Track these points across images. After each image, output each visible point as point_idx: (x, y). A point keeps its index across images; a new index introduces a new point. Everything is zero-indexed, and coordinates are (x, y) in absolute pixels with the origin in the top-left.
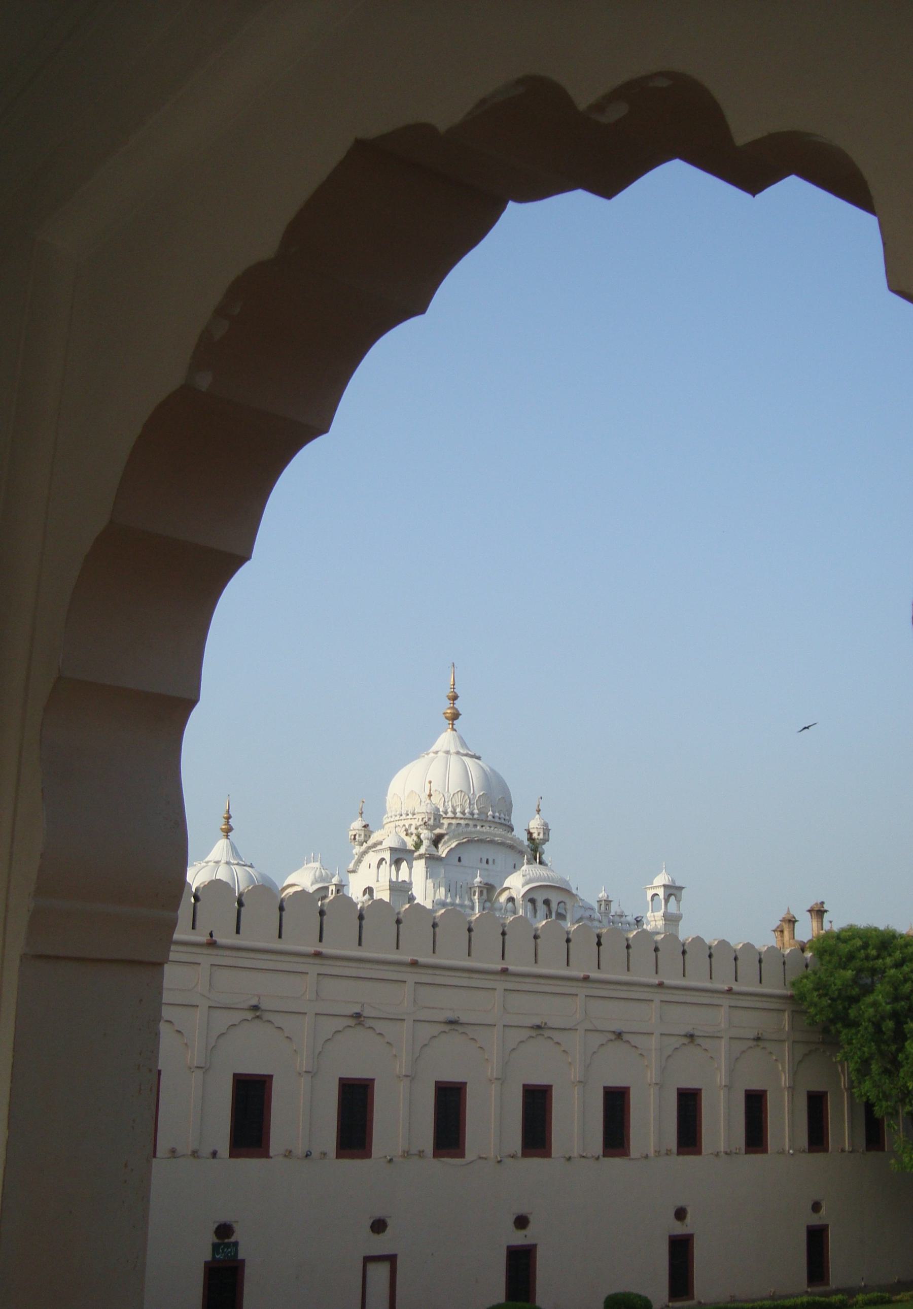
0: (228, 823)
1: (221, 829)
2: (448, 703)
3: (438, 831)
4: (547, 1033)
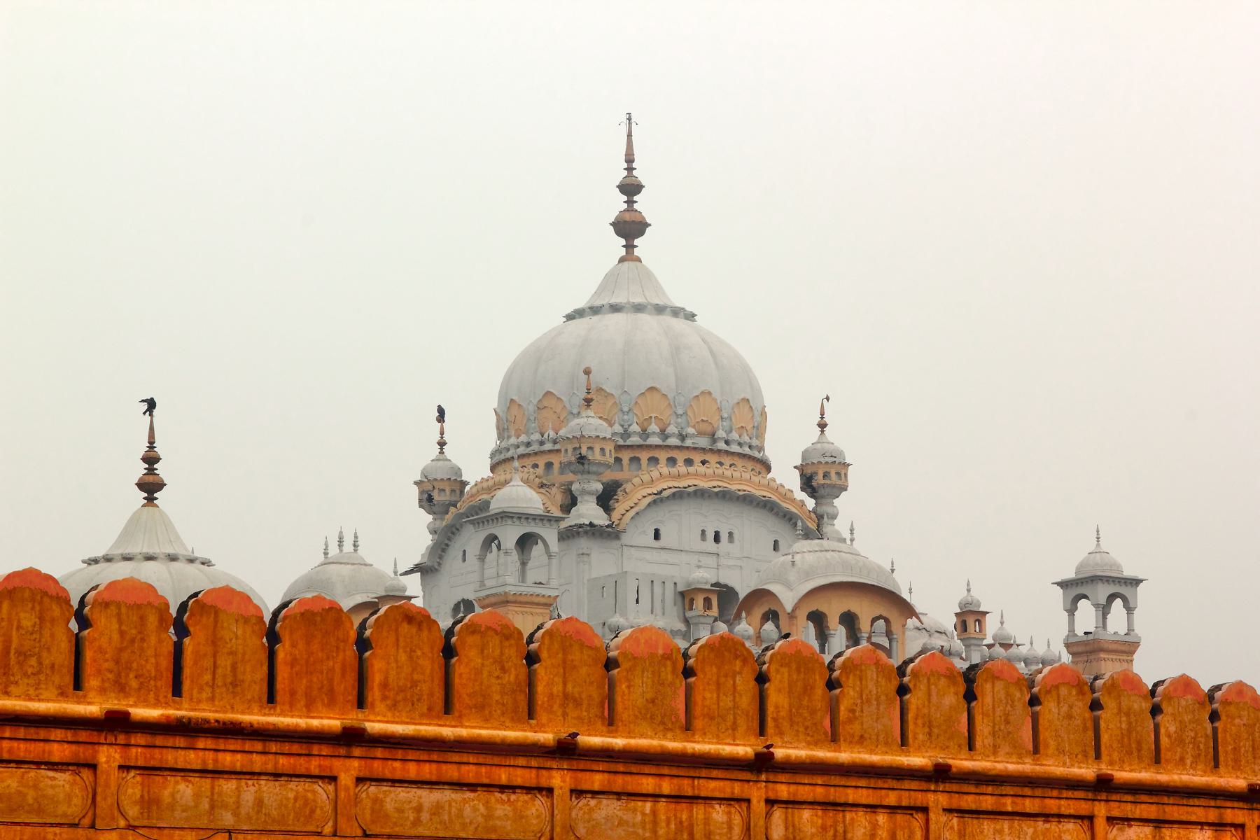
0: (151, 471)
2: (620, 202)
3: (610, 476)
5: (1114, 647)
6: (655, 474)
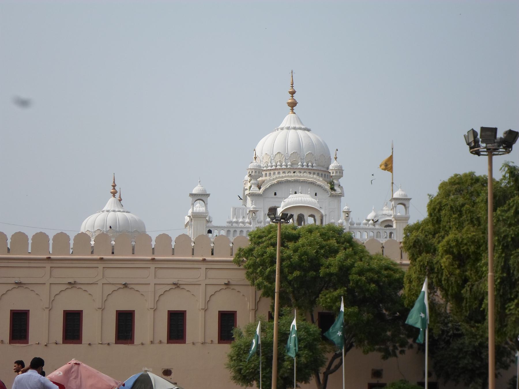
0: (114, 189)
1: (111, 192)
4: (78, 286)
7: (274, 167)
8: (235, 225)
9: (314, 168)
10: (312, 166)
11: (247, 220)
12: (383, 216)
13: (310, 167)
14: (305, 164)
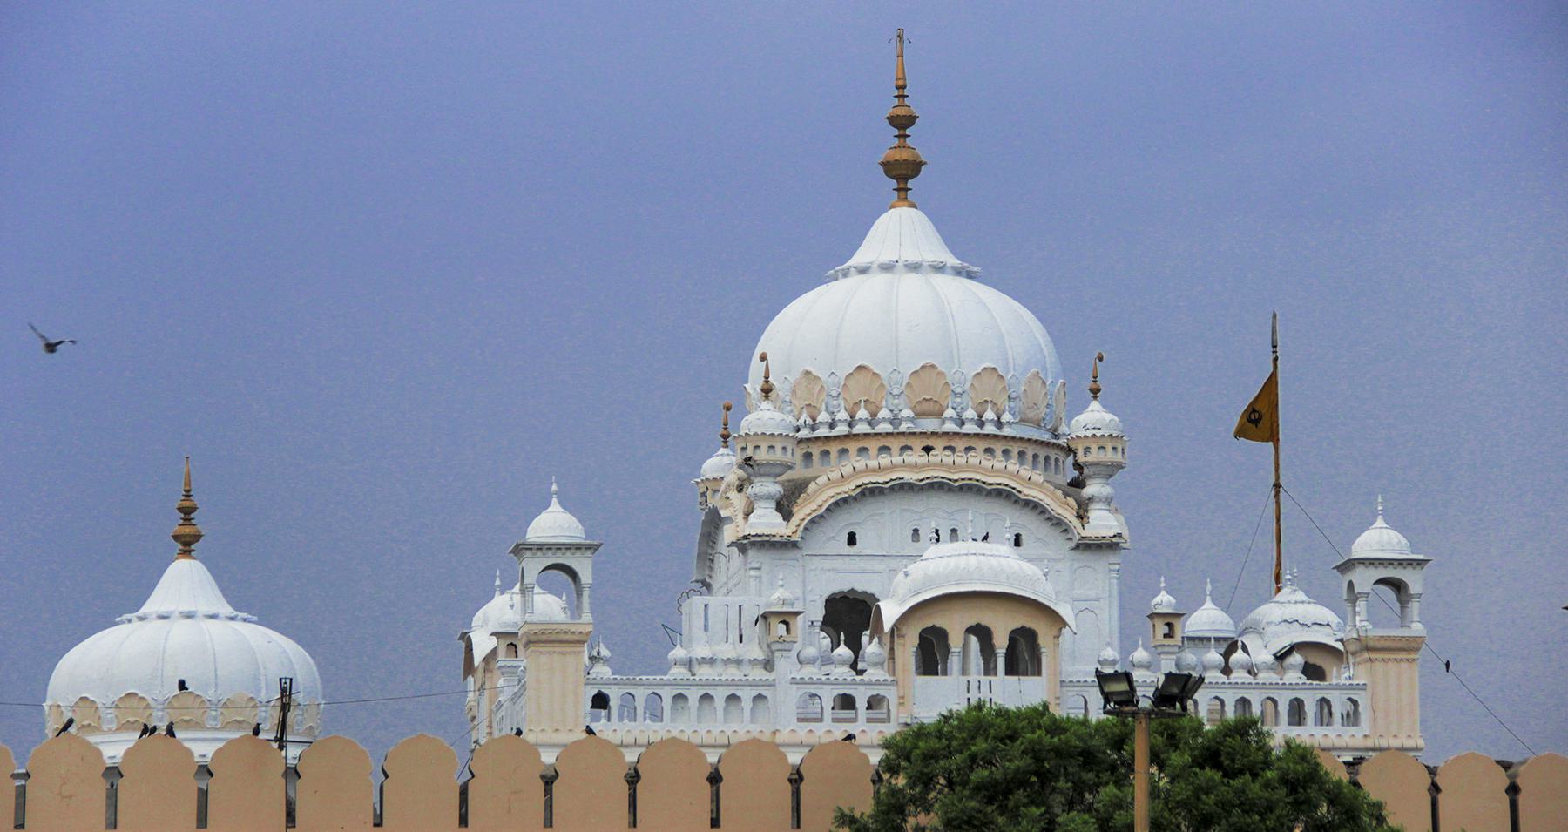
0: (187, 521)
1: (176, 537)
5: (1383, 644)
6: (848, 470)
7: (842, 429)
8: (704, 672)
9: (1007, 431)
10: (999, 424)
11: (759, 654)
12: (1285, 626)
13: (990, 429)
14: (970, 414)
